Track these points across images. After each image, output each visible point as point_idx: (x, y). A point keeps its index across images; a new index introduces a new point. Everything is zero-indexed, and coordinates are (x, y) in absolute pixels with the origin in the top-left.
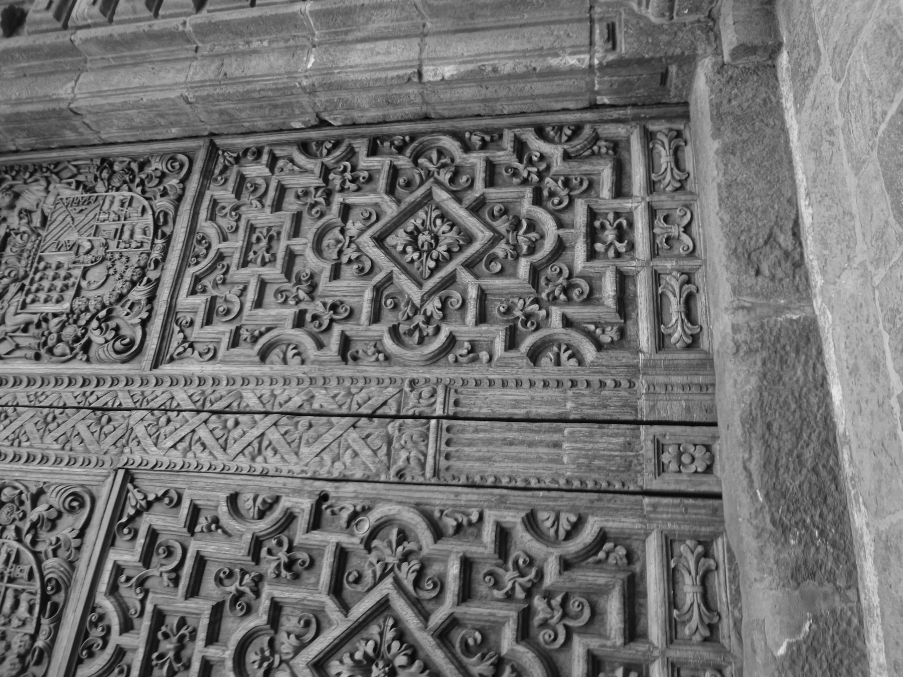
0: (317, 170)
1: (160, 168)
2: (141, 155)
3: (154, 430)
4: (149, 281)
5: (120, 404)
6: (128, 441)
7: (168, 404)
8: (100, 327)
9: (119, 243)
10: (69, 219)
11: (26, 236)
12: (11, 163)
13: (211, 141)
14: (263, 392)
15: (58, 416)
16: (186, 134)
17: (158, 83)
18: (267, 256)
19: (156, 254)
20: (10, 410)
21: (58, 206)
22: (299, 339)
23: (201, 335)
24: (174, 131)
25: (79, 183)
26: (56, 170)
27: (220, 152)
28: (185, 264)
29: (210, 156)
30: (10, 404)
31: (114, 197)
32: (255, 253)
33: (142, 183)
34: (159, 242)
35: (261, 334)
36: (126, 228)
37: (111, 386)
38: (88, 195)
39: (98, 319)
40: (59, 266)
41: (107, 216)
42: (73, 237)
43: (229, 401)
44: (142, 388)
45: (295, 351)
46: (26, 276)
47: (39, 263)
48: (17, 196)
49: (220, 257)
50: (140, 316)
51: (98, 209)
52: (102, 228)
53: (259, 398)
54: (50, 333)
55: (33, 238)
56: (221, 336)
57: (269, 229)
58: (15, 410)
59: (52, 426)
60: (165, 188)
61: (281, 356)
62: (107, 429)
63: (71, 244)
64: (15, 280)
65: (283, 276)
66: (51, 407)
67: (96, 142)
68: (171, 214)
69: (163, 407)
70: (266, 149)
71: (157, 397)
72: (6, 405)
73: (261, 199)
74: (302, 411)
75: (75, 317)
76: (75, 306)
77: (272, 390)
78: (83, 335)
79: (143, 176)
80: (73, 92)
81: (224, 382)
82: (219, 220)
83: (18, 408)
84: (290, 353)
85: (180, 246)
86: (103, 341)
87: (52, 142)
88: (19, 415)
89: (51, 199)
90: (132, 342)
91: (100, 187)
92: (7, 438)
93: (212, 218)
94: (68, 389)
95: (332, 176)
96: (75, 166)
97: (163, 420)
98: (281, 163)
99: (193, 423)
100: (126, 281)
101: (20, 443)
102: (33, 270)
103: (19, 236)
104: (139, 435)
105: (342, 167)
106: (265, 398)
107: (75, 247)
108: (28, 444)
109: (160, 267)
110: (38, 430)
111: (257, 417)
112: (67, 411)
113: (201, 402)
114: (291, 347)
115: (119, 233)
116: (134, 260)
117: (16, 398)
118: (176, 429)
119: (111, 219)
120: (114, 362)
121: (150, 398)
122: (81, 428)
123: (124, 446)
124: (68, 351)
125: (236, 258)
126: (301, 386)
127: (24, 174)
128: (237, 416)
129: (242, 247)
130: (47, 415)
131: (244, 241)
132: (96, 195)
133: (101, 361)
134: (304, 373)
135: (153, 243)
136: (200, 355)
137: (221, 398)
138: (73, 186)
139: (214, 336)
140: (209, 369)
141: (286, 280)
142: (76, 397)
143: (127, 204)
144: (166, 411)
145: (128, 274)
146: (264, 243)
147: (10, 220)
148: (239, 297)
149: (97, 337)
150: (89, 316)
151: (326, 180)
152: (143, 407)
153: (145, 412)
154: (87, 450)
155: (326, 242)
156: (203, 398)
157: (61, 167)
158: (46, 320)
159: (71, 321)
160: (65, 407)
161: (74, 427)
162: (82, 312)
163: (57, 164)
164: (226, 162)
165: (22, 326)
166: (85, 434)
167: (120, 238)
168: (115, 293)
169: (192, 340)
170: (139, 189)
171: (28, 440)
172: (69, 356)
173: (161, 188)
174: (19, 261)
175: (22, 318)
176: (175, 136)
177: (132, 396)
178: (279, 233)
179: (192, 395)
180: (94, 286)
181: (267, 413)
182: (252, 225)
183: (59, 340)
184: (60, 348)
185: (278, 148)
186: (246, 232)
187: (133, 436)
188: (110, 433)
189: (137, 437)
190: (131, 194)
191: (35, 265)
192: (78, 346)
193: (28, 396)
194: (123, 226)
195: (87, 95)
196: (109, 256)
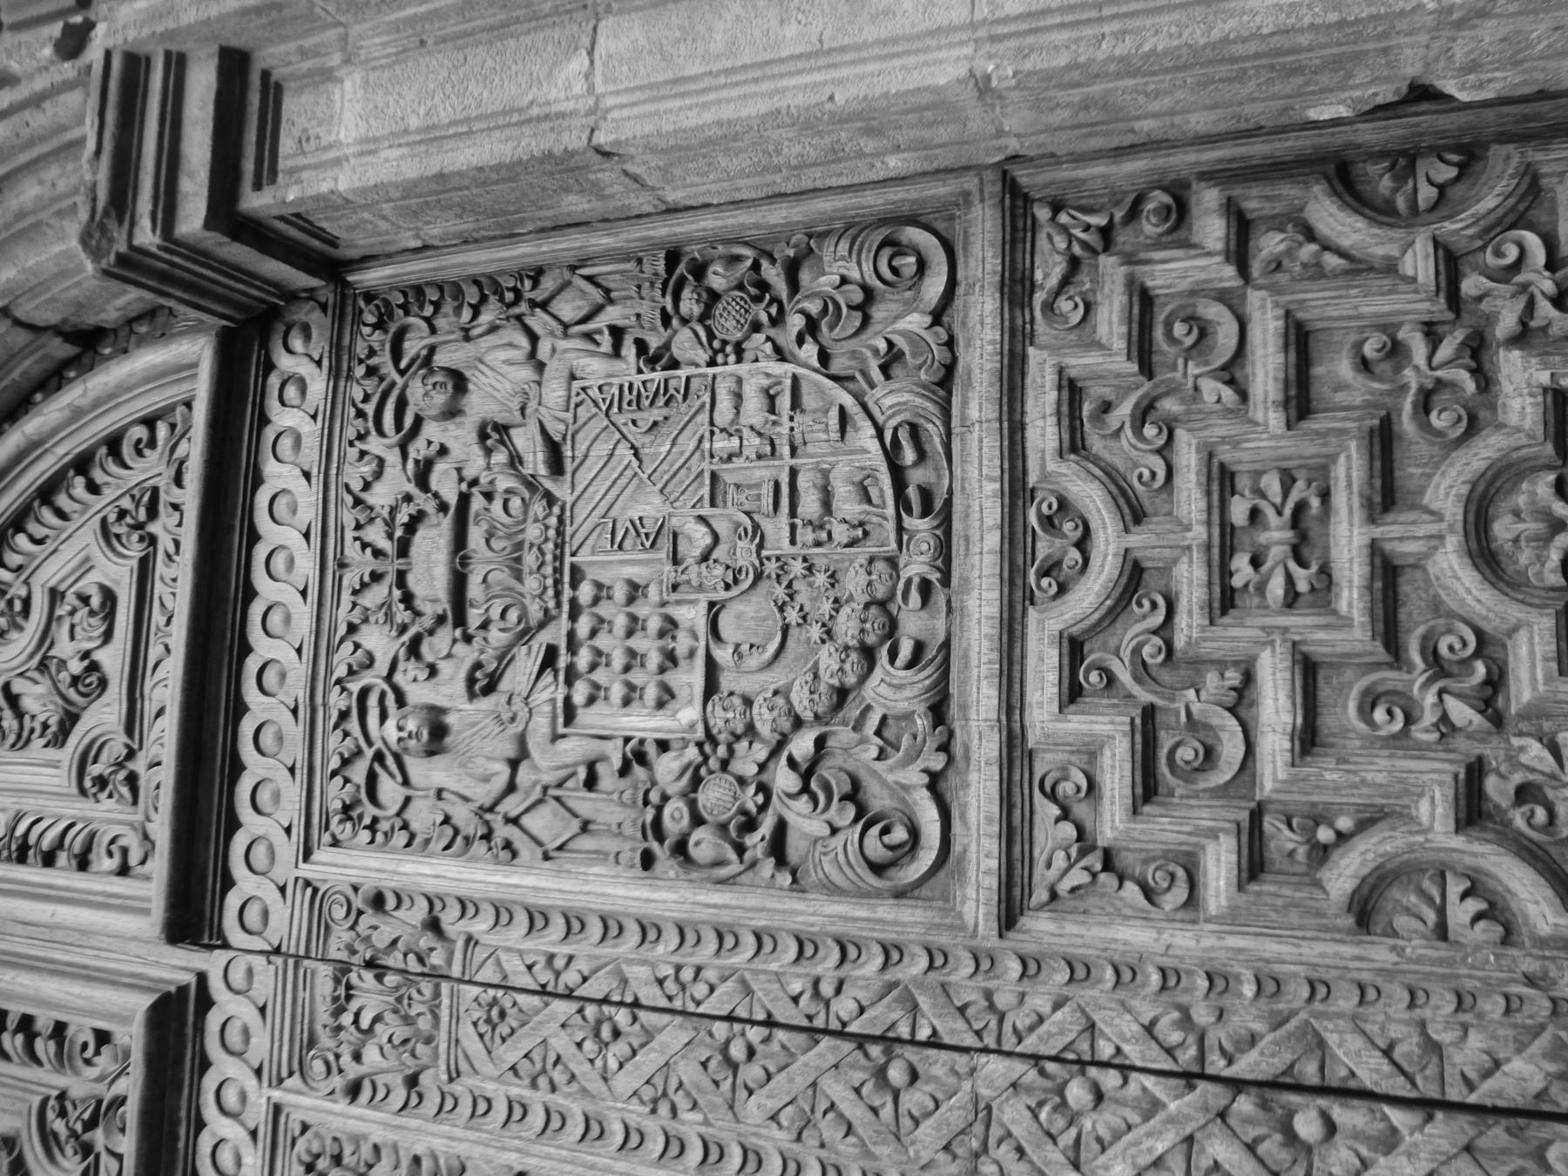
0: (1420, 263)
1: (854, 274)
2: (783, 234)
3: (1060, 1122)
4: (919, 648)
5: (935, 1032)
6: (985, 1143)
7: (1084, 1046)
8: (805, 789)
9: (793, 528)
10: (624, 452)
11: (515, 503)
12: (413, 280)
13: (1005, 173)
14: (1395, 1031)
15: (760, 1048)
16: (927, 167)
17: (871, 33)
18: (1303, 579)
19: (917, 566)
20: (622, 1017)
21: (583, 413)
22: (1484, 864)
23: (1136, 835)
24: (895, 164)
25: (617, 333)
26: (539, 295)
27: (1043, 213)
28: (1019, 594)
29: (1014, 228)
30: (616, 998)
31: (740, 381)
32: (1256, 562)
33: (812, 327)
34: (920, 526)
35: (1342, 837)
36: (803, 482)
37: (885, 965)
38: (658, 376)
39: (792, 763)
40: (635, 591)
41: (735, 442)
42: (650, 507)
43: (1288, 1057)
44: (981, 982)
45: (1474, 905)
46: (547, 619)
47: (574, 585)
48: (459, 382)
49: (1134, 576)
50: (920, 764)
51: (704, 417)
52: (729, 478)
53: (1387, 1053)
54: (665, 798)
55: (538, 508)
56: (1203, 841)
57: (1288, 481)
58: (635, 1019)
59: (751, 1073)
60: (890, 344)
61: (1431, 916)
62: (914, 1100)
63: (651, 528)
64: (525, 634)
65: (1378, 646)
66: (730, 1018)
67: (648, 209)
68: (933, 433)
69: (1071, 1056)
70: (1208, 199)
71: (1041, 1019)
72: (605, 1001)
73: (1233, 373)
74: (1546, 1107)
75: (722, 751)
76: (717, 723)
77: (1422, 1025)
78: (762, 808)
79: (814, 307)
80: (591, 89)
81: (1249, 990)
82: (1096, 443)
83: (642, 1015)
84: (1461, 913)
85: (993, 540)
86: (827, 831)
87: (522, 222)
88: (649, 1034)
89: (554, 392)
90: (914, 833)
91: (685, 343)
92: (635, 1093)
93: (1075, 445)
94: (758, 965)
95: (1471, 285)
96: (590, 279)
97: (1077, 1093)
98: (1270, 244)
99: (1187, 1118)
100: (847, 648)
101: (674, 1111)
102: (566, 607)
103: (497, 506)
104: (1017, 1131)
105: (1512, 253)
106: (1408, 1047)
107: (664, 538)
108: (699, 1117)
109: (939, 597)
110: (716, 1083)
111: (1397, 1116)
112: (781, 1035)
113: (1192, 1051)
114: (1455, 887)
115: (787, 494)
116: (854, 582)
117: (624, 982)
118: (1129, 1128)
119: (749, 452)
120: (878, 894)
121: (1023, 1022)
122: (835, 1089)
123: (977, 1156)
124: (732, 855)
125: (1191, 581)
126: (1519, 1018)
127: (458, 311)
128: (1322, 1102)
129: (1209, 547)
130: (728, 1042)
131: (1209, 523)
132: (682, 373)
133: (832, 889)
134: (1530, 981)
135: (900, 529)
136: (1149, 893)
137: (1253, 1040)
138: (606, 342)
139: (1183, 838)
140: (1186, 942)
141: (1387, 658)
142: (796, 1000)
143: (784, 402)
144: (1082, 1064)
145: (847, 627)
146: (1276, 535)
147: (456, 451)
148: (1232, 710)
149: (805, 822)
150: (761, 752)
151: (1454, 300)
152: (1006, 1047)
153: (1019, 1067)
154: (868, 1154)
155: (1503, 529)
156: (1191, 1039)
157: (548, 284)
158: (641, 757)
159: (713, 763)
160: (770, 1023)
161: (814, 1084)
162: (738, 738)
163: (537, 275)
164: (1077, 249)
165: (582, 773)
166: (852, 1109)
167: (793, 513)
168: (823, 688)
169: (1101, 842)
170: (809, 351)
171: (695, 1106)
172: (735, 868)
173: (882, 346)
174: (518, 576)
175: (573, 749)
176: (892, 174)
177: (962, 1010)
178: (1325, 495)
179: (1154, 1022)
180: (754, 661)
181: (1427, 1106)
182: (1222, 466)
183: (697, 820)
184: (704, 844)
185: (1256, 190)
186: (1208, 493)
187: (996, 1132)
188: (928, 1115)
189: (1009, 1134)
190: (789, 368)
191: (567, 593)
192: (756, 841)
193: (660, 982)
194: (794, 473)
195: (638, 96)
196: (771, 567)
